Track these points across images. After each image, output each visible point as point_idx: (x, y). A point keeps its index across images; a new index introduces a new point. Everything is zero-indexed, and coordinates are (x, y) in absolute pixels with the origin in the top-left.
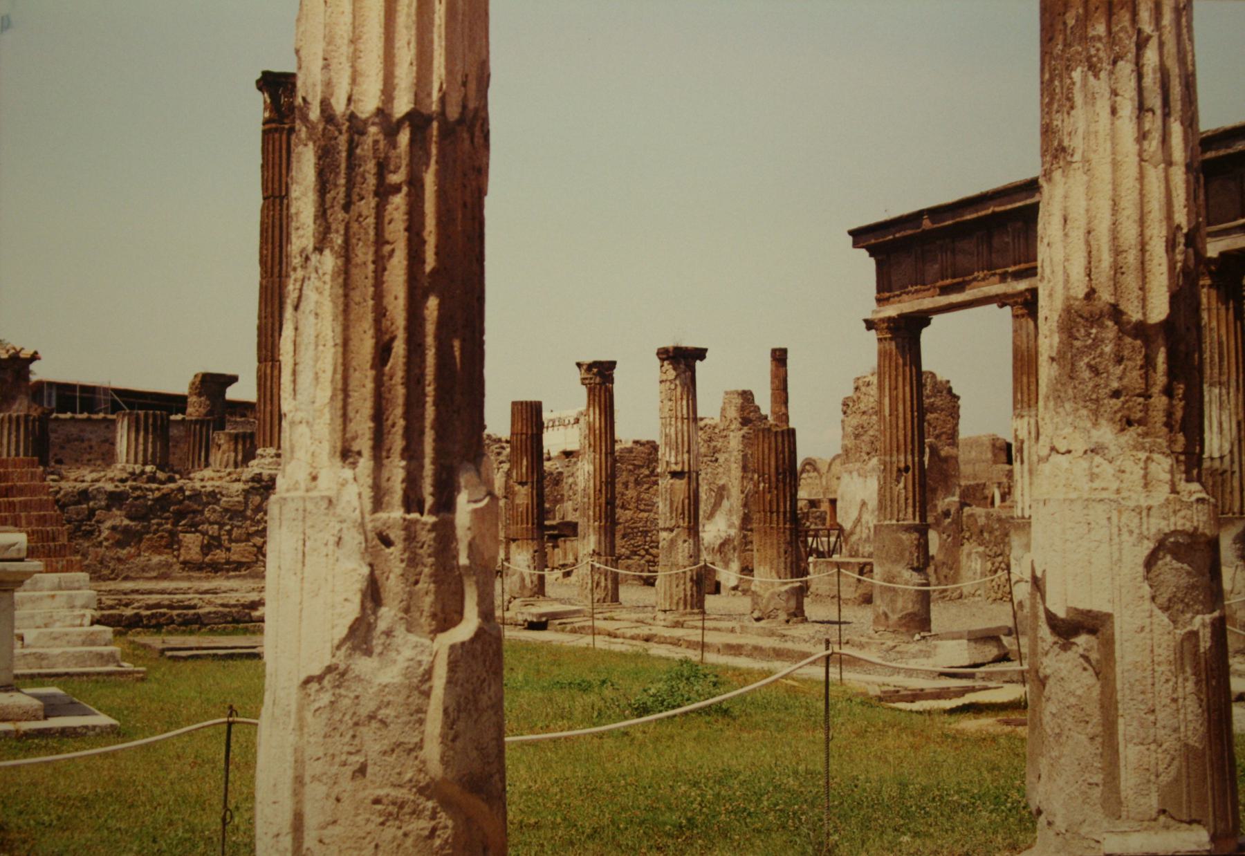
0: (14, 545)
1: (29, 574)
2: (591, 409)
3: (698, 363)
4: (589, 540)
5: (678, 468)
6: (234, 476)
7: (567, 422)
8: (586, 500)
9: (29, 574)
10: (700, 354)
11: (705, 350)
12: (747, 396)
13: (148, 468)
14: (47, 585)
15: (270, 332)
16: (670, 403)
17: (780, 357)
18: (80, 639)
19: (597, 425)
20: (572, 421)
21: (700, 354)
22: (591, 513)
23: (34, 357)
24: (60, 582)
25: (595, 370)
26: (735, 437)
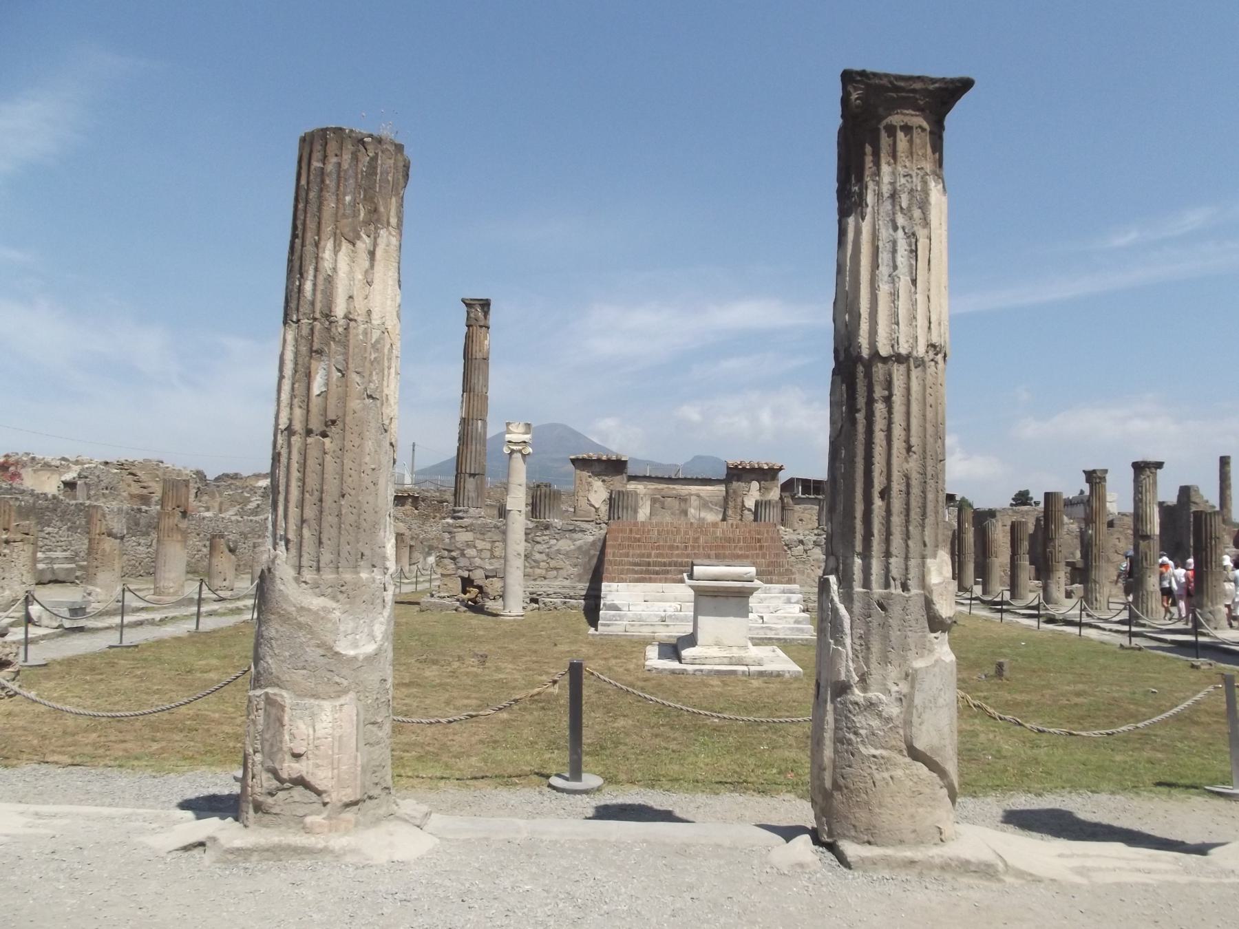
1: (756, 589)
9: (756, 589)
14: (776, 591)
17: (1224, 462)
18: (793, 620)
21: (1159, 465)
23: (781, 469)
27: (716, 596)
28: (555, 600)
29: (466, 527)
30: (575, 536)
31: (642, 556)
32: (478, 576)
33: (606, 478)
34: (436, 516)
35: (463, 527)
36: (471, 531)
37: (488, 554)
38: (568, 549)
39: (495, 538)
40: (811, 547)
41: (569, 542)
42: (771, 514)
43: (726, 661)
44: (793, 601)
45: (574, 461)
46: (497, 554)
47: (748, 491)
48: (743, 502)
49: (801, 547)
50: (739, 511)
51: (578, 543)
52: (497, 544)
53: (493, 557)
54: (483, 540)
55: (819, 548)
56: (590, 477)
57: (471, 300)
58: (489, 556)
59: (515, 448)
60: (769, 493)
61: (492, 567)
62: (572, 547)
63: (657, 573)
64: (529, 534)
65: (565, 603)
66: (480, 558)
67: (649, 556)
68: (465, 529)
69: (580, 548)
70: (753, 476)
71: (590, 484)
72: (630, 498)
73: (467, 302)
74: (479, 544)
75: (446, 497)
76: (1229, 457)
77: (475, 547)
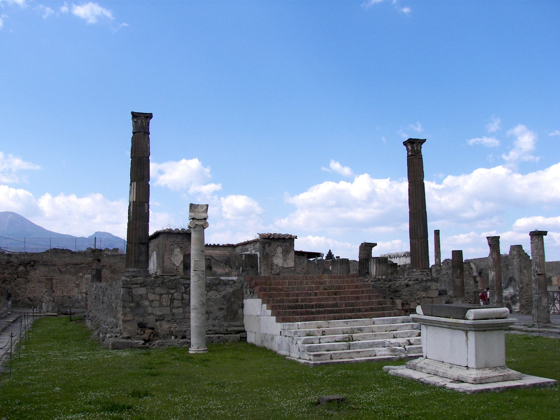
0: (506, 312)
2: (493, 253)
3: (544, 236)
4: (495, 297)
5: (540, 273)
6: (408, 279)
7: (400, 256)
8: (493, 284)
10: (545, 233)
11: (547, 232)
12: (520, 247)
13: (383, 277)
14: (399, 321)
15: (416, 229)
16: (537, 250)
19: (496, 258)
20: (402, 256)
21: (545, 233)
22: (495, 288)
24: (403, 320)
25: (494, 239)
26: (516, 261)
27: (485, 331)
28: (212, 336)
29: (140, 284)
30: (221, 288)
31: (293, 301)
32: (150, 320)
33: (183, 245)
34: (5, 273)
35: (137, 284)
36: (144, 286)
37: (156, 304)
38: (216, 298)
39: (163, 291)
41: (217, 292)
43: (500, 378)
44: (415, 327)
46: (164, 304)
47: (275, 254)
48: (272, 260)
50: (270, 267)
51: (223, 293)
52: (164, 296)
53: (161, 305)
54: (154, 293)
56: (172, 245)
58: (158, 305)
60: (289, 255)
61: (161, 313)
62: (218, 296)
65: (219, 337)
66: (152, 307)
67: (297, 301)
68: (140, 286)
69: (224, 297)
70: (278, 243)
71: (172, 251)
74: (151, 297)
75: (12, 259)
76: (439, 230)
77: (147, 299)
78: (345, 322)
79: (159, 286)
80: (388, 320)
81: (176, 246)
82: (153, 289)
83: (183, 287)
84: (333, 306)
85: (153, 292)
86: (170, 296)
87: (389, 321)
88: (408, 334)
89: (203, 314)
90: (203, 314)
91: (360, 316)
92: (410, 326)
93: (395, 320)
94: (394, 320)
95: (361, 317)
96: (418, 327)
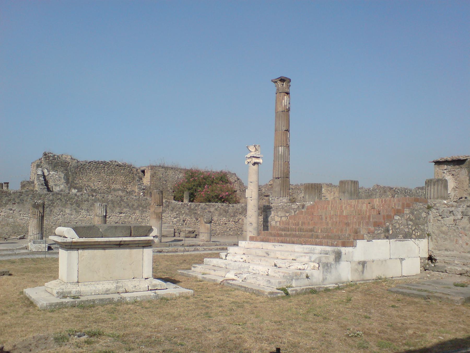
14: (317, 251)
24: (321, 250)
39: (282, 215)
40: (460, 217)
42: (432, 190)
44: (312, 260)
45: (438, 163)
49: (452, 218)
54: (278, 216)
55: (467, 218)
56: (444, 173)
57: (276, 79)
59: (249, 160)
63: (281, 236)
64: (296, 212)
72: (347, 186)
73: (274, 81)
78: (274, 245)
79: (280, 210)
80: (307, 248)
81: (448, 174)
82: (277, 212)
83: (293, 211)
84: (311, 230)
85: (277, 215)
86: (286, 218)
87: (308, 250)
88: (286, 264)
89: (250, 231)
90: (250, 231)
91: (301, 242)
92: (308, 257)
93: (314, 250)
94: (312, 249)
95: (302, 242)
96: (315, 260)
